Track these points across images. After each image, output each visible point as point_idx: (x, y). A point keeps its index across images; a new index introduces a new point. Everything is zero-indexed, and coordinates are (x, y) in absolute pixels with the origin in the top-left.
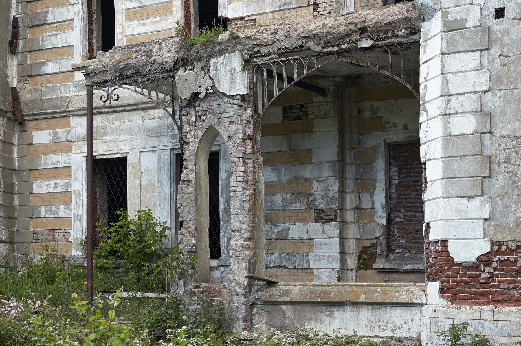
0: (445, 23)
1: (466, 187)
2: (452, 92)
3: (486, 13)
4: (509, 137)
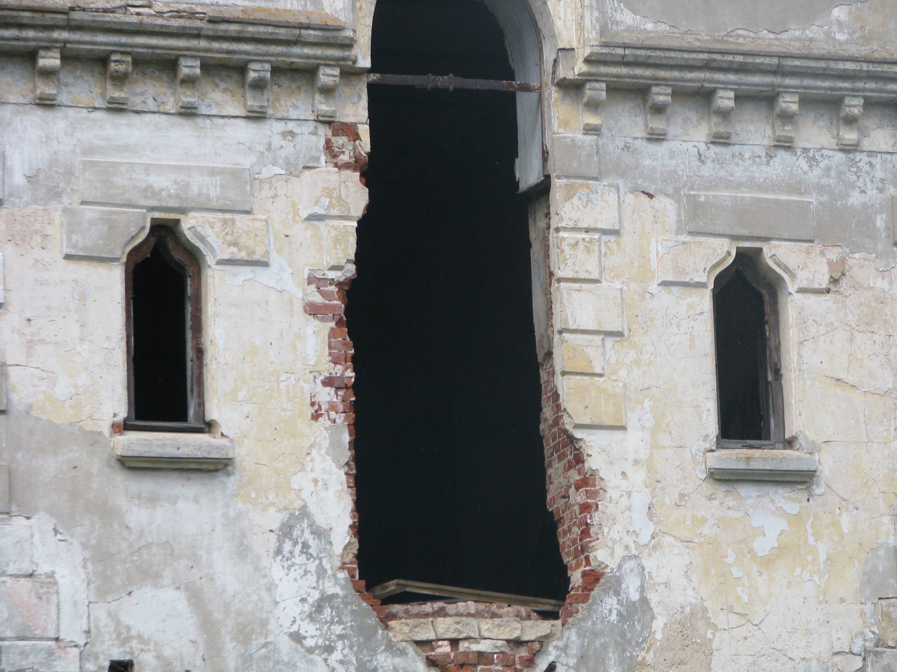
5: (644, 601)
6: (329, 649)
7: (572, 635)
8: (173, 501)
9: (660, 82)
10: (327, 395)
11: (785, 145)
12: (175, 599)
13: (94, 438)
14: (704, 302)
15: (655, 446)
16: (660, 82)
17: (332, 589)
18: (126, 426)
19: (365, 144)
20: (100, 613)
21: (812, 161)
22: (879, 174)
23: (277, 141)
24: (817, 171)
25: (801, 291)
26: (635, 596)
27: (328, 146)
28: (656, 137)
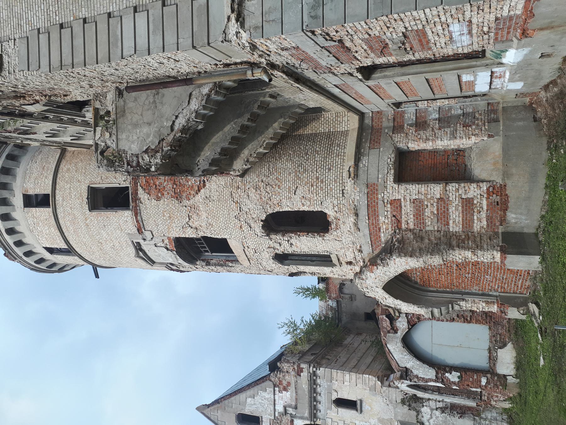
14: (340, 409)
15: (358, 420)
21: (322, 391)
28: (320, 412)
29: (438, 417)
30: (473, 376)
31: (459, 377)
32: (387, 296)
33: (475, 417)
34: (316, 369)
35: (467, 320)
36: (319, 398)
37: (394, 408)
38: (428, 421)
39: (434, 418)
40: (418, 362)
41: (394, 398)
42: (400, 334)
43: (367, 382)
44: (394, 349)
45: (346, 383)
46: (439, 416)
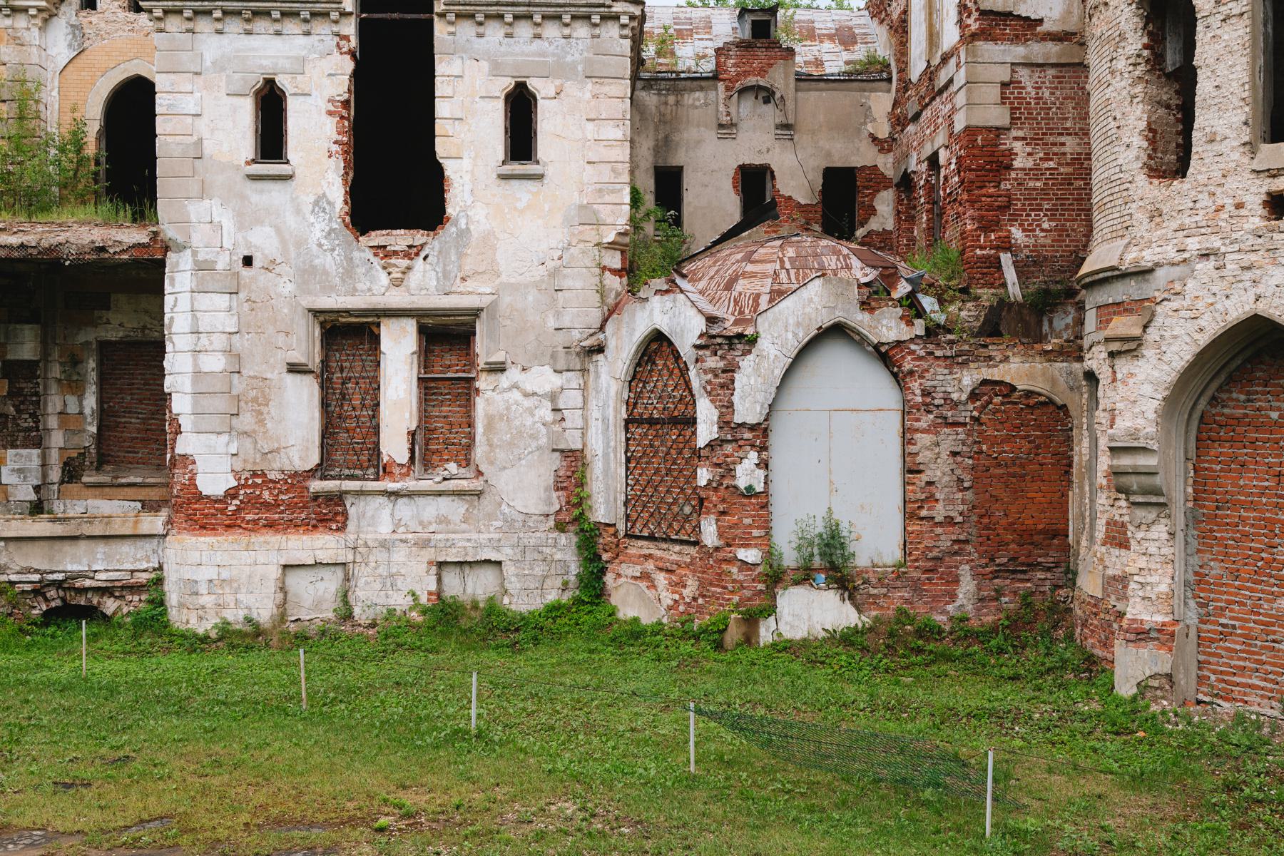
0: (196, 262)
1: (215, 422)
2: (201, 330)
3: (235, 258)
4: (255, 377)
5: (468, 229)
6: (333, 250)
7: (436, 243)
8: (270, 192)
9: (479, 12)
10: (335, 148)
11: (537, 36)
12: (268, 230)
13: (238, 168)
16: (479, 12)
17: (335, 226)
18: (254, 161)
19: (354, 43)
20: (239, 236)
21: (550, 43)
22: (581, 48)
23: (316, 44)
24: (553, 47)
25: (542, 98)
26: (464, 227)
27: (338, 45)
28: (480, 36)
29: (533, 415)
30: (758, 528)
31: (750, 488)
32: (1212, 326)
33: (552, 518)
34: (624, 26)
35: (920, 508)
36: (524, 30)
37: (537, 285)
38: (515, 386)
39: (528, 403)
40: (779, 373)
41: (567, 283)
42: (859, 319)
43: (608, 199)
44: (811, 301)
45: (590, 126)
46: (536, 419)
